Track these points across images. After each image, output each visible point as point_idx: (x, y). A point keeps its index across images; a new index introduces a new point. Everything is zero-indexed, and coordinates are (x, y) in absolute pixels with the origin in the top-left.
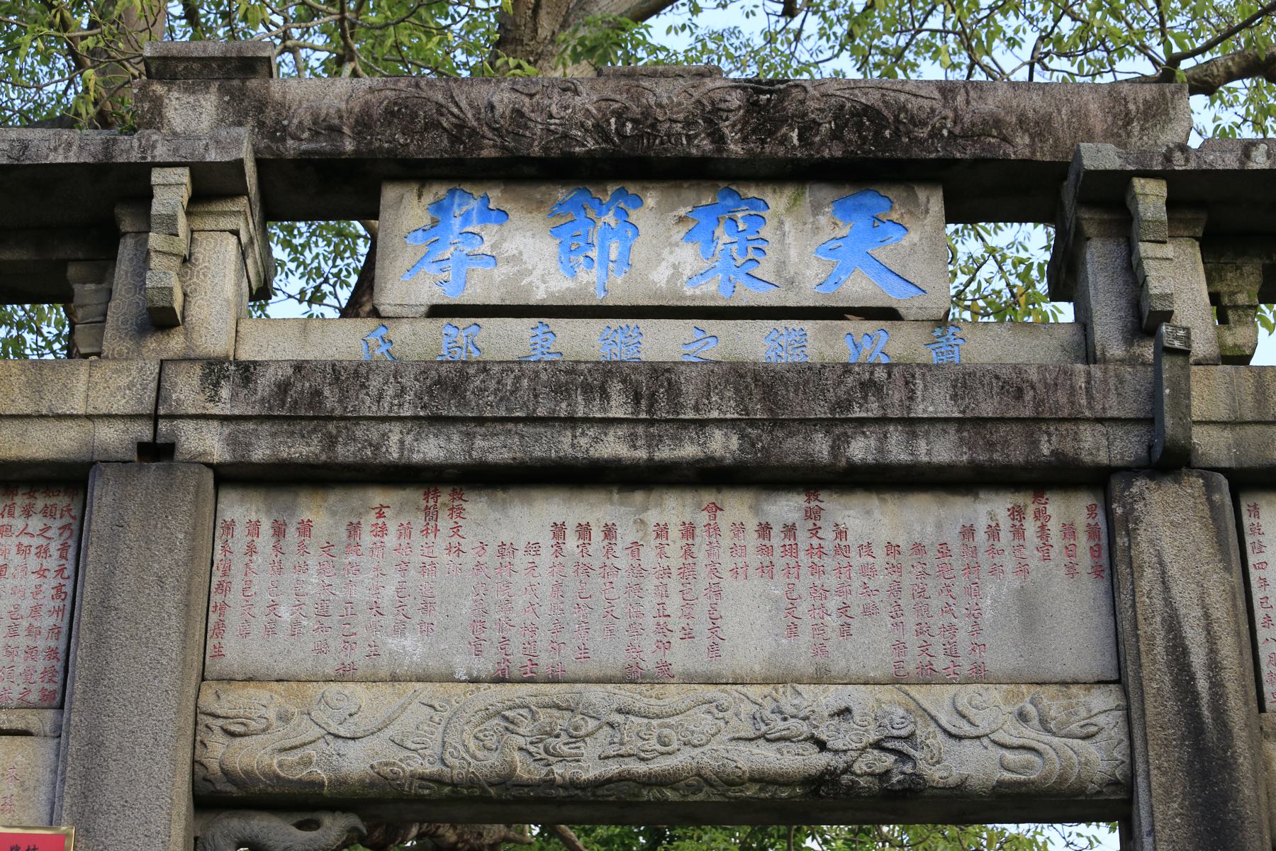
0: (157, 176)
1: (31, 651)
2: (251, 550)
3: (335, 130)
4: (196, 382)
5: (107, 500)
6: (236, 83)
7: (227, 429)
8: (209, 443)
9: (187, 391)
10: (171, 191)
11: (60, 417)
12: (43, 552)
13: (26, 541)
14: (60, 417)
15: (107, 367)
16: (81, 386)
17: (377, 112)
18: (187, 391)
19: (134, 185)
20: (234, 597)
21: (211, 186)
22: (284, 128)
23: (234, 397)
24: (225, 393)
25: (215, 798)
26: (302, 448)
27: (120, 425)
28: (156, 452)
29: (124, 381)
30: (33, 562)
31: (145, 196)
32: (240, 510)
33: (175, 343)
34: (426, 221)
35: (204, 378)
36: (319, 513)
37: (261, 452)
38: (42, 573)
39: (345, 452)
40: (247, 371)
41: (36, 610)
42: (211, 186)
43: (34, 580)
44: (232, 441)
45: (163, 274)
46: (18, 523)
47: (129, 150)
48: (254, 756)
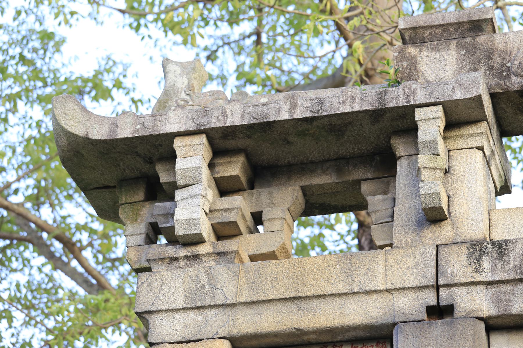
0: (419, 114)
4: (464, 258)
6: (469, 40)
7: (492, 291)
8: (478, 302)
9: (457, 266)
10: (430, 124)
11: (368, 293)
14: (368, 293)
15: (396, 255)
16: (380, 269)
18: (457, 266)
19: (403, 123)
21: (458, 118)
22: (509, 69)
23: (493, 267)
24: (486, 264)
27: (411, 295)
28: (440, 312)
29: (411, 262)
31: (411, 130)
33: (444, 232)
35: (470, 255)
40: (501, 248)
42: (458, 118)
44: (496, 300)
45: (431, 184)
47: (396, 98)
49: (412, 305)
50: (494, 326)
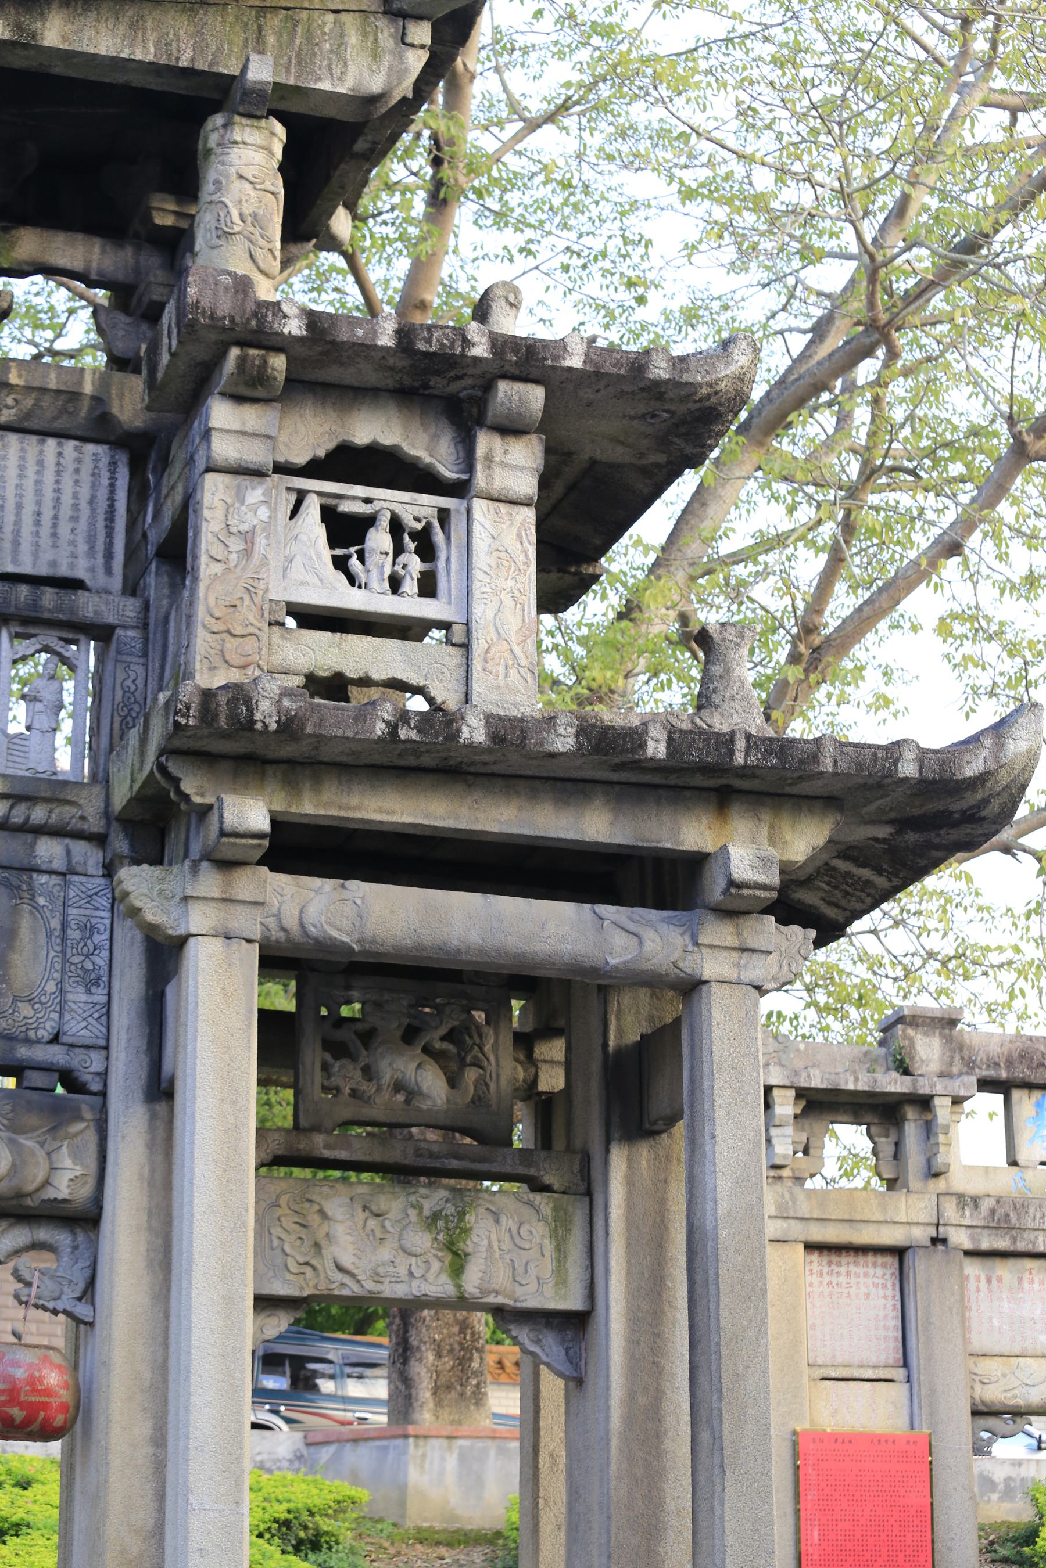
0: (937, 1101)
1: (886, 1338)
2: (978, 1290)
3: (997, 1064)
4: (954, 1206)
5: (922, 1267)
6: (947, 1031)
7: (969, 1231)
8: (960, 1238)
9: (950, 1211)
11: (895, 1223)
12: (884, 1287)
13: (876, 1280)
14: (895, 1223)
15: (914, 1197)
16: (903, 1207)
17: (1015, 1055)
18: (950, 1211)
20: (973, 1313)
22: (974, 1062)
23: (971, 1215)
24: (967, 1213)
25: (976, 1413)
26: (1002, 1243)
27: (922, 1228)
29: (922, 1205)
30: (881, 1293)
32: (973, 1269)
33: (941, 1184)
34: (1033, 1113)
35: (958, 1204)
36: (1004, 1270)
37: (985, 1245)
38: (885, 1297)
39: (1021, 1246)
40: (976, 1201)
41: (886, 1316)
43: (882, 1301)
44: (972, 1238)
46: (871, 1271)
48: (993, 1394)
49: (921, 1235)
50: (968, 1253)
